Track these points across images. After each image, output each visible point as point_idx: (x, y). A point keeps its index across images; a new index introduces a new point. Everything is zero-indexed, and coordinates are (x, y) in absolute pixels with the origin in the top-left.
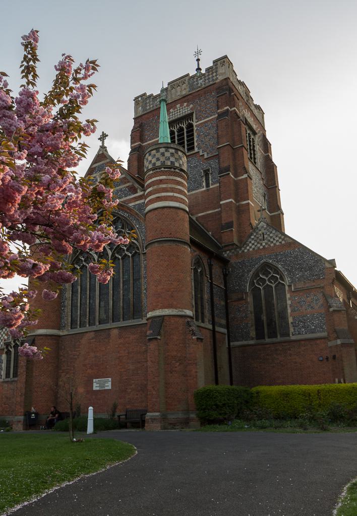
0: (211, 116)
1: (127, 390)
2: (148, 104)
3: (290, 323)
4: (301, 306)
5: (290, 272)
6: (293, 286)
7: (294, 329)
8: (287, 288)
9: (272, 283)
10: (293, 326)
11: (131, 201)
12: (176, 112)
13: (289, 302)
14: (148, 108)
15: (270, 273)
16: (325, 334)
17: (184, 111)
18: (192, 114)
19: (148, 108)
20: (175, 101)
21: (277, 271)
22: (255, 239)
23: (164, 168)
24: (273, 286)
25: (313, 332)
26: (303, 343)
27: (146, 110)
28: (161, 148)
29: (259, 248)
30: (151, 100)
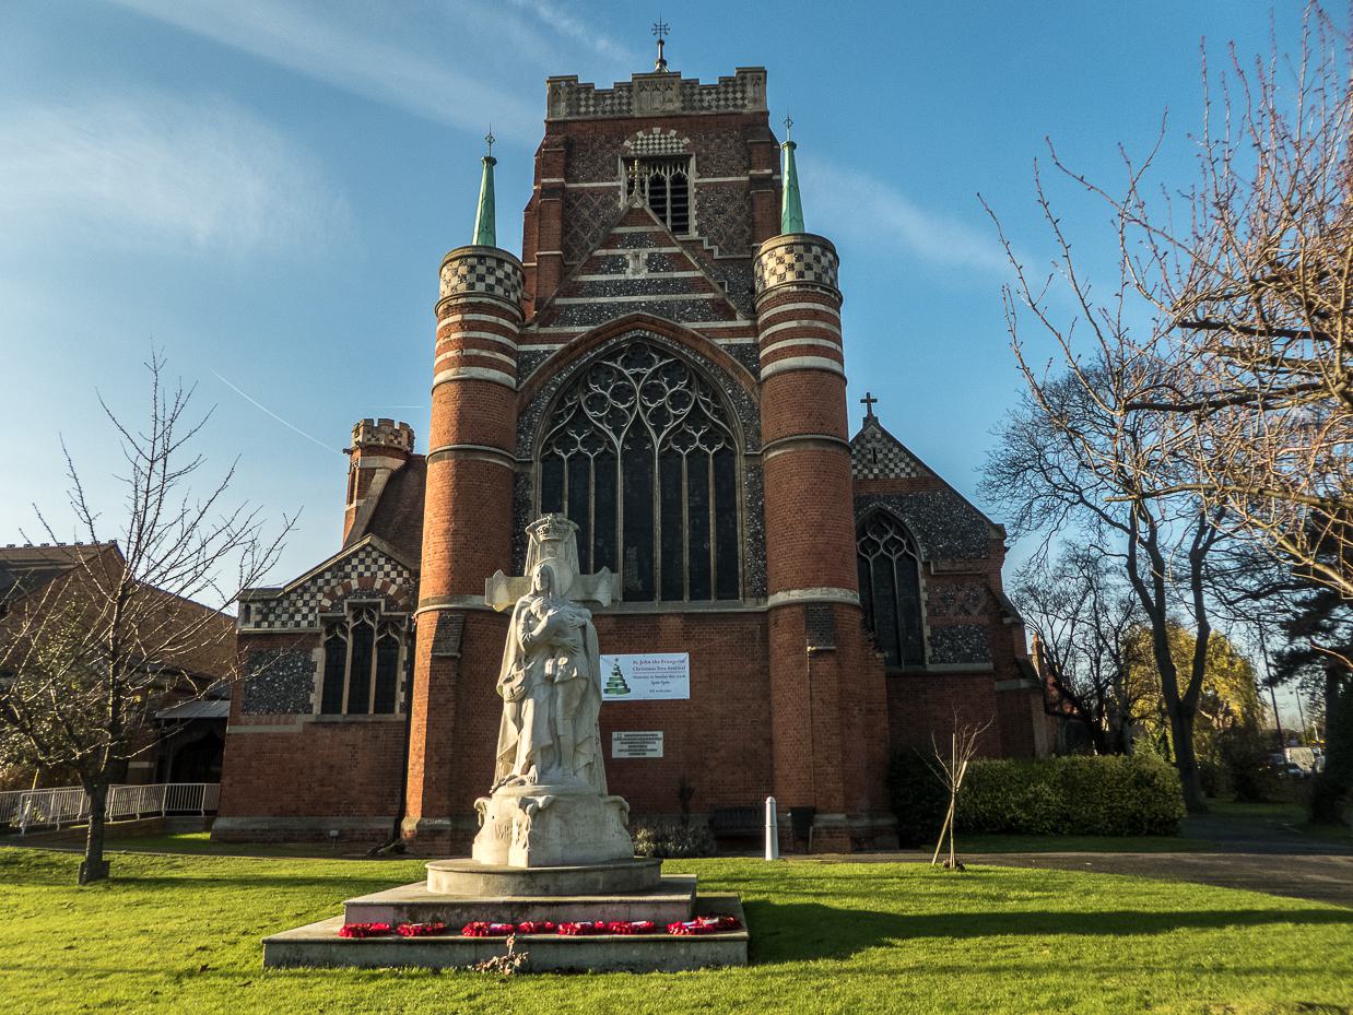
0: (730, 175)
2: (583, 103)
3: (925, 637)
4: (948, 607)
5: (926, 537)
6: (932, 565)
7: (934, 651)
8: (920, 566)
9: (890, 552)
10: (932, 644)
12: (651, 141)
13: (924, 596)
14: (583, 110)
15: (887, 532)
16: (988, 666)
17: (669, 146)
18: (687, 158)
19: (583, 110)
20: (651, 118)
21: (901, 529)
22: (860, 456)
23: (822, 288)
24: (894, 559)
25: (968, 659)
26: (949, 679)
27: (578, 113)
28: (814, 245)
29: (866, 476)
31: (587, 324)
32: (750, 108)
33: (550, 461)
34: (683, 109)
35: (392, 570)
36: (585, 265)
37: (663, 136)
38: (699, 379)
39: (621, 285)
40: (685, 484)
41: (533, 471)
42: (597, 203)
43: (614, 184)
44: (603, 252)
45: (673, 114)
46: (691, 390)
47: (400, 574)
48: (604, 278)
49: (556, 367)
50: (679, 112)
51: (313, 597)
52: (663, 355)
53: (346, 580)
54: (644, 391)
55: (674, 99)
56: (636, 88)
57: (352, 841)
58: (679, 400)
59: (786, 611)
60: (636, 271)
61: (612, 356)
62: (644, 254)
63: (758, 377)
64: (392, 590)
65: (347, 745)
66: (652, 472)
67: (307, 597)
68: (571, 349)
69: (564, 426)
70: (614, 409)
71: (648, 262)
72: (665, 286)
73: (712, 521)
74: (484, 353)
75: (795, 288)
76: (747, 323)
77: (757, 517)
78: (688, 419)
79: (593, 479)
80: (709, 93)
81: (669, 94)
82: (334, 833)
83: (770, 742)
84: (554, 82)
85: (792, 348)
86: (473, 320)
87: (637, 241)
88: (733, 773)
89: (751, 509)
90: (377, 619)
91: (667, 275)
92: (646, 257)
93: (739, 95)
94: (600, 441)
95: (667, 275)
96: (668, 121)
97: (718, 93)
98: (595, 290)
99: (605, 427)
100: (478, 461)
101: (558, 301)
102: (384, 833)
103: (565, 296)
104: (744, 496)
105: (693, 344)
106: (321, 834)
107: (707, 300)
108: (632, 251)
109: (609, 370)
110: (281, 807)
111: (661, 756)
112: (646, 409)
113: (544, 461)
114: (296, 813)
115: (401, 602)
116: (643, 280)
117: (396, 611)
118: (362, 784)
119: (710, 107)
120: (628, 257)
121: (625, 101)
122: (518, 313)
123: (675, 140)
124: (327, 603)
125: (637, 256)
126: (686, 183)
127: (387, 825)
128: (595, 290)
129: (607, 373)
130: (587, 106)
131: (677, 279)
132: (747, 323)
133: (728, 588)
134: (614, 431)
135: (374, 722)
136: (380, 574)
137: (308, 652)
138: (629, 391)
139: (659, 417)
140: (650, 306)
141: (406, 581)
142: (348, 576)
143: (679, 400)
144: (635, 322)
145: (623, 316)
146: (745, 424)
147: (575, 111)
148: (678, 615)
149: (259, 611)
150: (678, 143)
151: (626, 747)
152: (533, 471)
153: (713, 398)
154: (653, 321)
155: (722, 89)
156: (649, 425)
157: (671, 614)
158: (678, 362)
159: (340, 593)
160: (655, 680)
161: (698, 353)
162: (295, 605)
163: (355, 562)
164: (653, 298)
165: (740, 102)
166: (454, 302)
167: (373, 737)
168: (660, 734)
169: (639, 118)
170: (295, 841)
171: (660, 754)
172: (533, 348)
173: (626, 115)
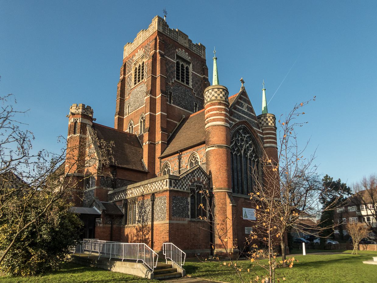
35: (204, 176)
47: (206, 178)
51: (187, 181)
53: (194, 177)
64: (204, 183)
67: (185, 181)
75: (274, 128)
76: (261, 131)
124: (190, 183)
132: (261, 131)
136: (201, 177)
137: (187, 198)
140: (248, 119)
141: (207, 180)
142: (194, 176)
149: (174, 183)
159: (193, 181)
162: (183, 183)
163: (196, 172)
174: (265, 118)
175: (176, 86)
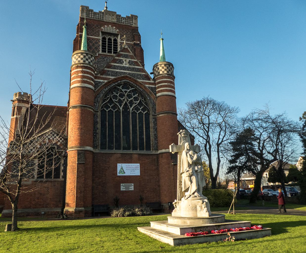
1: (144, 191)
11: (147, 83)
18: (118, 35)
23: (173, 76)
27: (89, 17)
28: (171, 65)
30: (93, 13)
31: (113, 76)
32: (134, 25)
33: (103, 112)
34: (117, 22)
36: (113, 60)
37: (112, 28)
38: (141, 94)
39: (122, 67)
40: (138, 120)
41: (98, 114)
42: (94, 42)
43: (99, 38)
44: (117, 58)
45: (115, 23)
46: (139, 97)
47: (61, 139)
48: (118, 65)
49: (105, 86)
50: (116, 22)
52: (132, 87)
54: (127, 95)
55: (115, 19)
56: (105, 14)
57: (48, 215)
58: (136, 99)
59: (165, 154)
60: (126, 64)
61: (119, 85)
62: (128, 60)
63: (156, 96)
64: (59, 144)
65: (46, 187)
66: (129, 117)
68: (109, 82)
69: (107, 102)
70: (119, 99)
71: (129, 62)
72: (133, 69)
73: (144, 130)
74: (88, 80)
75: (167, 75)
76: (153, 82)
77: (155, 130)
78: (138, 104)
79: (114, 118)
80: (124, 19)
81: (113, 17)
82: (43, 213)
83: (159, 186)
84: (82, 7)
85: (166, 90)
86: (85, 71)
87: (126, 56)
88: (151, 194)
89: (154, 128)
90: (54, 151)
91: (134, 67)
92: (128, 61)
93: (131, 21)
94: (116, 107)
95: (134, 67)
96: (113, 24)
97: (126, 20)
98: (115, 67)
99: (117, 104)
100: (87, 110)
101: (106, 69)
102: (58, 212)
103: (107, 68)
104: (152, 125)
105: (140, 85)
106: (39, 213)
107: (144, 75)
108: (125, 59)
109: (118, 89)
110: (25, 206)
111: (133, 190)
112: (128, 100)
113: (101, 111)
114: (30, 207)
115: (61, 147)
116: (127, 67)
117: (60, 149)
118: (50, 199)
119: (124, 23)
120: (124, 60)
121: (102, 16)
122: (94, 69)
123: (115, 30)
125: (126, 60)
126: (117, 41)
127: (59, 210)
128: (115, 67)
129: (118, 90)
130: (92, 15)
131: (136, 68)
132: (153, 82)
133: (148, 148)
134: (119, 105)
135: (54, 181)
138: (123, 95)
139: (131, 103)
140: (129, 74)
141: (63, 141)
143: (136, 99)
144: (125, 77)
145: (123, 75)
146: (152, 107)
147: (88, 16)
148: (137, 154)
150: (115, 30)
151: (124, 188)
152: (98, 114)
153: (144, 99)
154: (130, 78)
155: (127, 19)
156: (129, 104)
157: (135, 154)
158: (136, 89)
160: (132, 170)
161: (141, 87)
164: (130, 72)
165: (131, 23)
166: (79, 65)
167: (53, 185)
168: (133, 184)
169: (105, 22)
170: (30, 216)
171: (133, 189)
172: (99, 80)
173: (102, 20)
174: (156, 68)
175: (100, 59)
